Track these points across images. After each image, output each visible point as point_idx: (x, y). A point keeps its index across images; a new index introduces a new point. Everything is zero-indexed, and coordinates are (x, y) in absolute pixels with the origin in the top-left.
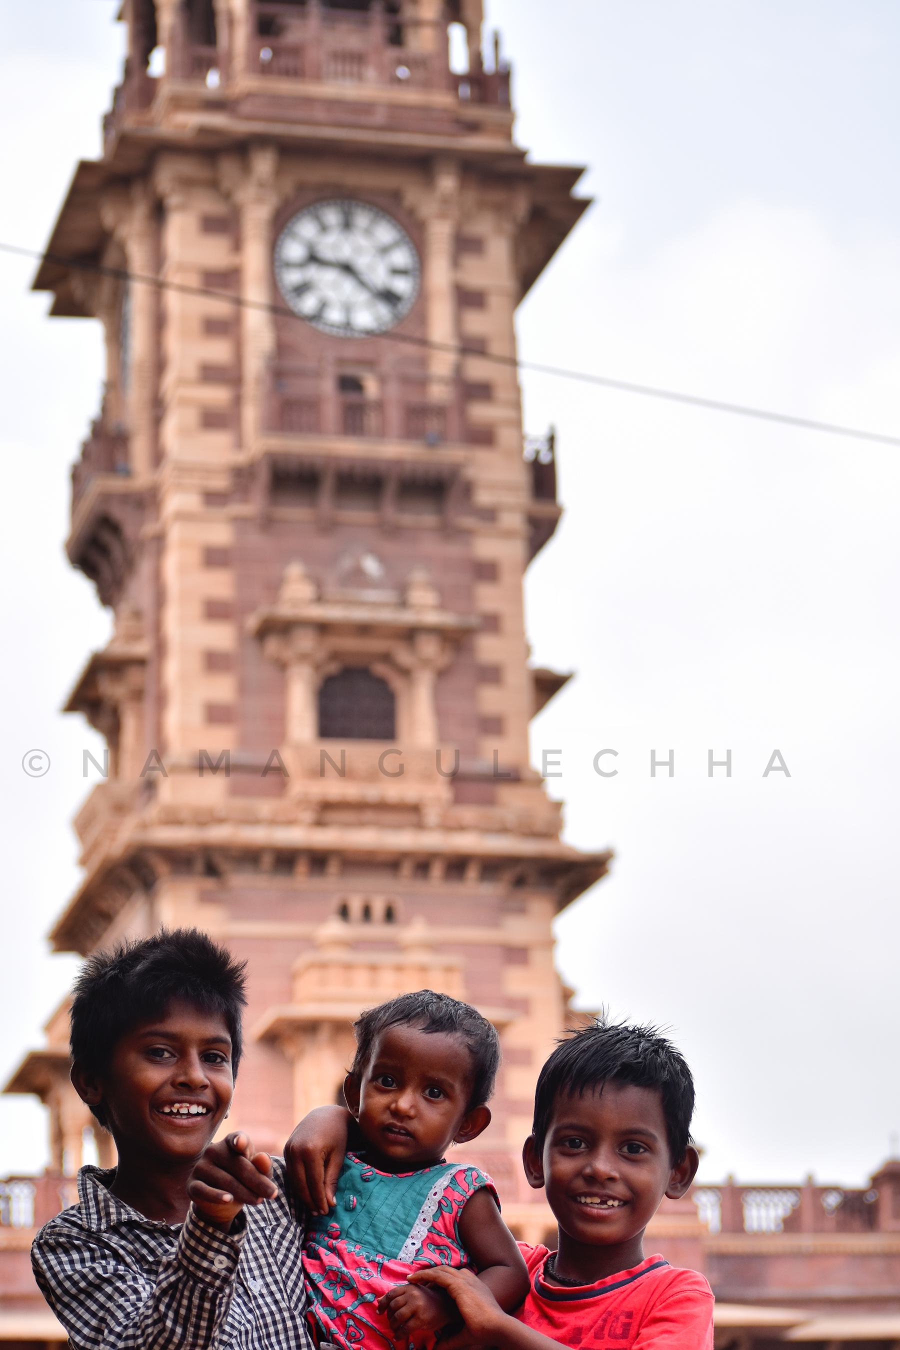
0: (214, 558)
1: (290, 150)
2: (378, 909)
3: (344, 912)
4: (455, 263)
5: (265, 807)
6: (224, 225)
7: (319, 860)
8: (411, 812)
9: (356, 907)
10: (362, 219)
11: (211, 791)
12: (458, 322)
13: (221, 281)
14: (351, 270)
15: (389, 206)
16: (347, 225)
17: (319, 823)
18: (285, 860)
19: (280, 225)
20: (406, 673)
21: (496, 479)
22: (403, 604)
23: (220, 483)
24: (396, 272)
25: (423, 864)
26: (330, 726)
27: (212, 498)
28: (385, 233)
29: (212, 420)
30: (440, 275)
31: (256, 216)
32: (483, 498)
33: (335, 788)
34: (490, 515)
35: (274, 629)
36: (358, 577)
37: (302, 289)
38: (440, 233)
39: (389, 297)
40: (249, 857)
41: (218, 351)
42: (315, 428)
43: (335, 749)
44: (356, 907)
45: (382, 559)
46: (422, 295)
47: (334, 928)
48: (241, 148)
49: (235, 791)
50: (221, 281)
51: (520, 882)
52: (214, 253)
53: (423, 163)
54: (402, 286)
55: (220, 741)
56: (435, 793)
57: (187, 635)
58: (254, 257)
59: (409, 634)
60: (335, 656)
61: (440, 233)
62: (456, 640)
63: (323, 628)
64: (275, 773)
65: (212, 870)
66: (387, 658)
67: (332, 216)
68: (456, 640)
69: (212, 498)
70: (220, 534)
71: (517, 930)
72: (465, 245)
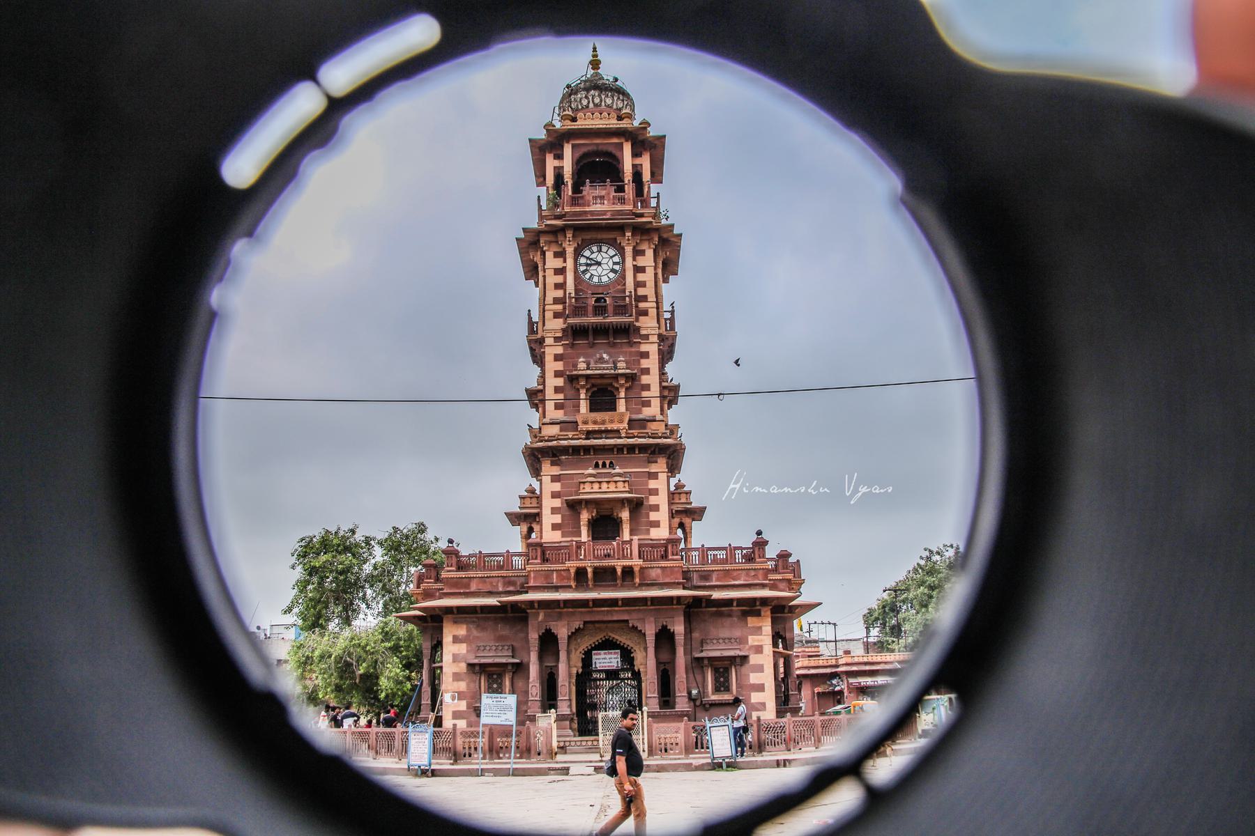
0: (557, 358)
1: (577, 229)
2: (608, 462)
3: (597, 466)
4: (634, 259)
5: (570, 434)
6: (561, 254)
7: (587, 449)
8: (616, 433)
9: (600, 463)
10: (604, 248)
11: (554, 430)
12: (635, 277)
15: (613, 243)
16: (600, 251)
17: (587, 439)
18: (576, 450)
19: (578, 253)
20: (617, 389)
21: (648, 324)
22: (616, 368)
23: (559, 335)
24: (615, 263)
25: (620, 449)
27: (557, 339)
28: (611, 252)
29: (557, 315)
31: (570, 250)
32: (643, 332)
33: (591, 427)
34: (647, 337)
35: (572, 379)
36: (601, 360)
37: (584, 272)
38: (629, 250)
39: (613, 271)
40: (565, 450)
41: (560, 293)
42: (586, 315)
43: (594, 415)
44: (600, 463)
45: (608, 354)
46: (624, 270)
48: (563, 230)
50: (561, 271)
51: (653, 453)
52: (558, 263)
53: (621, 228)
54: (617, 267)
55: (559, 415)
57: (553, 382)
58: (570, 263)
60: (593, 385)
61: (629, 250)
62: (632, 378)
63: (588, 377)
65: (554, 455)
66: (611, 385)
67: (595, 249)
68: (632, 378)
69: (557, 339)
70: (560, 350)
71: (653, 468)
72: (638, 253)
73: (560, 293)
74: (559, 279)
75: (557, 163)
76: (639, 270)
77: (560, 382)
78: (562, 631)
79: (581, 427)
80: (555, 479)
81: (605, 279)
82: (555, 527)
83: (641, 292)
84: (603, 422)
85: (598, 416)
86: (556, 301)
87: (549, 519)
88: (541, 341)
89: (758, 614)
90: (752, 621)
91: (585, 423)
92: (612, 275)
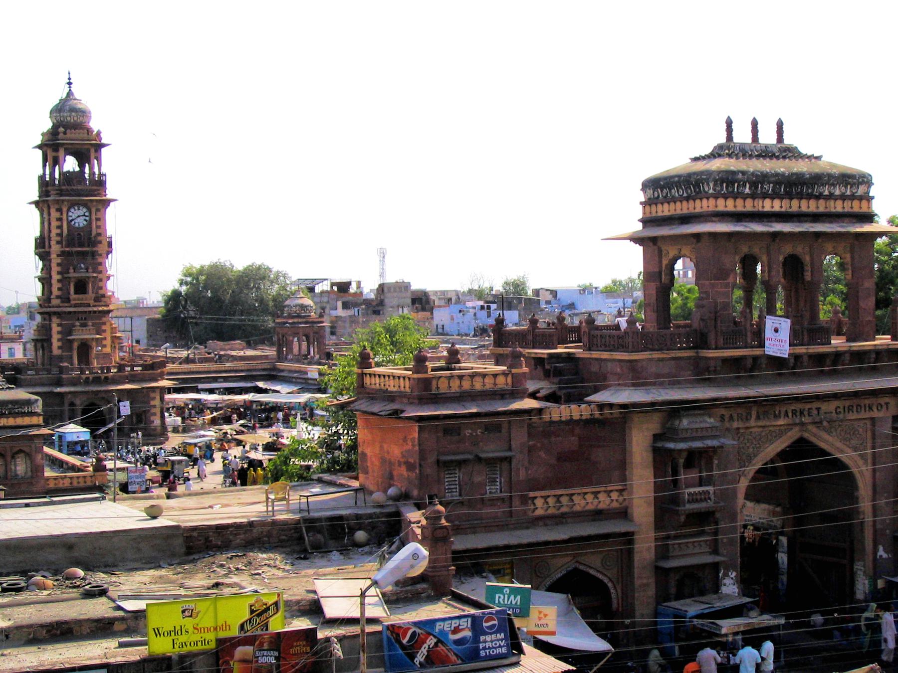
6: (59, 210)
13: (60, 219)
14: (78, 217)
19: (68, 210)
25: (90, 312)
26: (76, 293)
27: (58, 256)
28: (85, 210)
29: (58, 243)
30: (94, 217)
31: (65, 210)
41: (59, 231)
42: (74, 246)
47: (77, 323)
49: (62, 302)
52: (58, 215)
56: (92, 302)
59: (88, 277)
64: (68, 300)
70: (59, 261)
71: (104, 319)
73: (59, 231)
74: (59, 223)
75: (54, 154)
76: (98, 219)
77: (59, 277)
78: (78, 402)
79: (73, 302)
80: (59, 325)
81: (81, 225)
82: (59, 348)
83: (99, 231)
84: (82, 299)
85: (81, 296)
86: (58, 235)
87: (56, 344)
88: (49, 254)
89: (154, 392)
90: (152, 395)
91: (74, 300)
92: (85, 223)
